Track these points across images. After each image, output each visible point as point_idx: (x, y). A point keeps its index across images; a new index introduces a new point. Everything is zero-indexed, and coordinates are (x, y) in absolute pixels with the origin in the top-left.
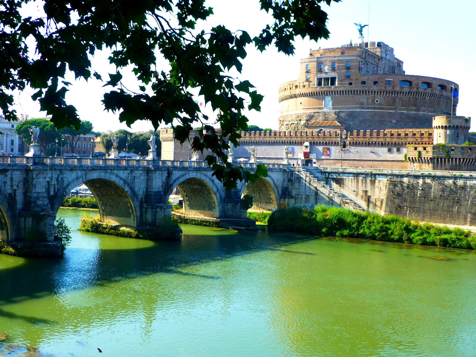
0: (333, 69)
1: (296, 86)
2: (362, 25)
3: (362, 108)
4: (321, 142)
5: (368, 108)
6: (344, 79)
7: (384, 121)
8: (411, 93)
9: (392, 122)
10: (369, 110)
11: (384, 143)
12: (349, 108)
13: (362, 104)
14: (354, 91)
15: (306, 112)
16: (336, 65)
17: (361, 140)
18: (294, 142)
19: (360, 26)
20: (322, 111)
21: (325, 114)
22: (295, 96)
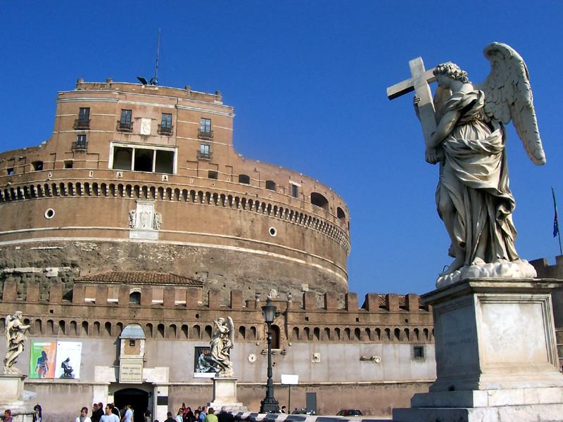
0: (165, 130)
1: (39, 165)
3: (242, 245)
4: (191, 326)
5: (254, 245)
6: (196, 160)
8: (328, 225)
11: (402, 329)
12: (207, 239)
13: (239, 232)
14: (223, 196)
15: (66, 239)
17: (333, 320)
18: (80, 322)
20: (127, 240)
21: (134, 250)
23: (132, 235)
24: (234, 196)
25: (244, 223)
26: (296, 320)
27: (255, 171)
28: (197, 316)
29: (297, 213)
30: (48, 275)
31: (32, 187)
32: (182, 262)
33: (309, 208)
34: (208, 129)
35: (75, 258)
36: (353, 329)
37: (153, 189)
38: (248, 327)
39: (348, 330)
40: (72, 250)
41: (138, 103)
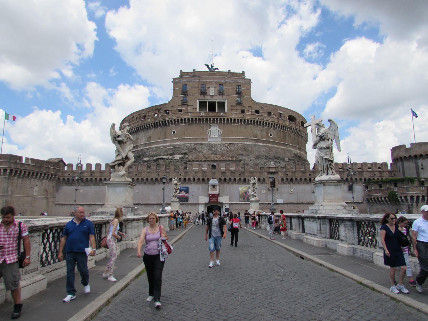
0: (221, 93)
2: (214, 68)
3: (257, 141)
4: (237, 179)
6: (235, 105)
7: (277, 158)
9: (284, 160)
10: (264, 144)
12: (242, 140)
14: (248, 120)
15: (182, 143)
16: (225, 88)
17: (299, 175)
18: (192, 179)
19: (212, 67)
20: (207, 142)
21: (211, 146)
22: (164, 124)
23: (209, 140)
24: (253, 120)
25: (258, 132)
26: (282, 175)
27: (262, 108)
28: (240, 175)
29: (282, 126)
30: (175, 159)
31: (165, 121)
32: (231, 151)
33: (288, 123)
34: (240, 90)
35: (186, 151)
36: (308, 179)
37: (217, 119)
38: (262, 179)
39: (305, 179)
40: (185, 148)
41: (208, 81)
